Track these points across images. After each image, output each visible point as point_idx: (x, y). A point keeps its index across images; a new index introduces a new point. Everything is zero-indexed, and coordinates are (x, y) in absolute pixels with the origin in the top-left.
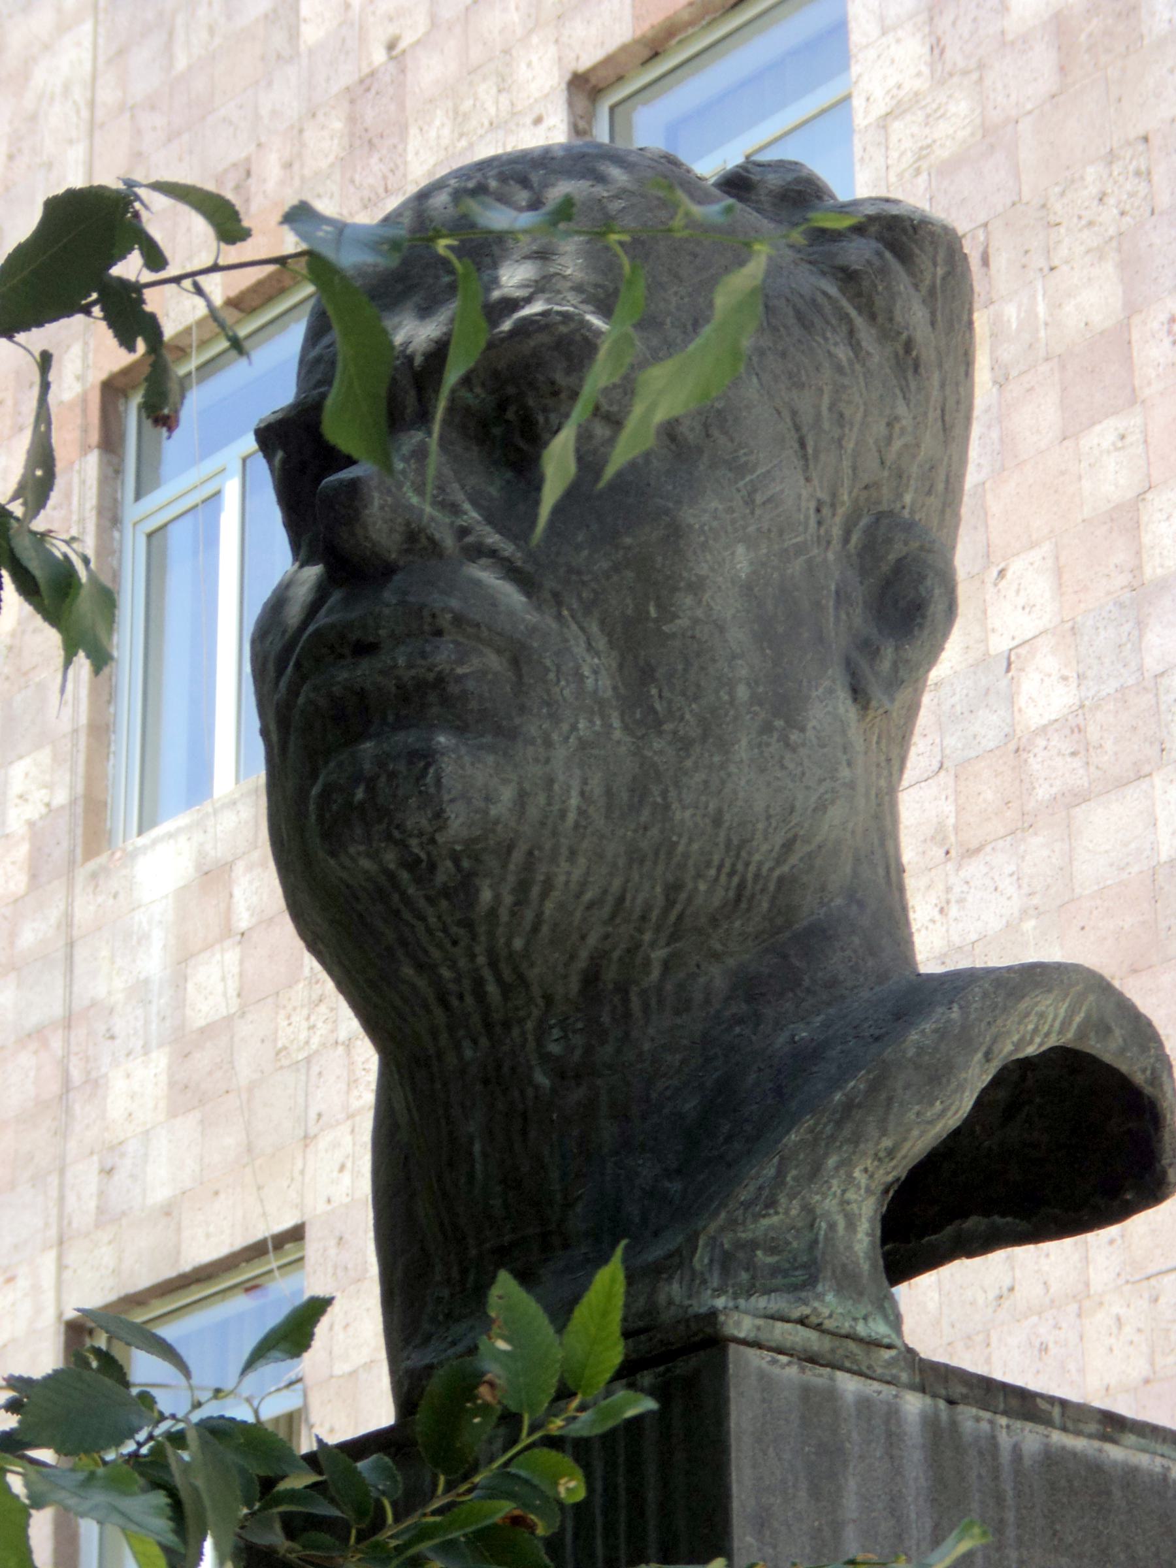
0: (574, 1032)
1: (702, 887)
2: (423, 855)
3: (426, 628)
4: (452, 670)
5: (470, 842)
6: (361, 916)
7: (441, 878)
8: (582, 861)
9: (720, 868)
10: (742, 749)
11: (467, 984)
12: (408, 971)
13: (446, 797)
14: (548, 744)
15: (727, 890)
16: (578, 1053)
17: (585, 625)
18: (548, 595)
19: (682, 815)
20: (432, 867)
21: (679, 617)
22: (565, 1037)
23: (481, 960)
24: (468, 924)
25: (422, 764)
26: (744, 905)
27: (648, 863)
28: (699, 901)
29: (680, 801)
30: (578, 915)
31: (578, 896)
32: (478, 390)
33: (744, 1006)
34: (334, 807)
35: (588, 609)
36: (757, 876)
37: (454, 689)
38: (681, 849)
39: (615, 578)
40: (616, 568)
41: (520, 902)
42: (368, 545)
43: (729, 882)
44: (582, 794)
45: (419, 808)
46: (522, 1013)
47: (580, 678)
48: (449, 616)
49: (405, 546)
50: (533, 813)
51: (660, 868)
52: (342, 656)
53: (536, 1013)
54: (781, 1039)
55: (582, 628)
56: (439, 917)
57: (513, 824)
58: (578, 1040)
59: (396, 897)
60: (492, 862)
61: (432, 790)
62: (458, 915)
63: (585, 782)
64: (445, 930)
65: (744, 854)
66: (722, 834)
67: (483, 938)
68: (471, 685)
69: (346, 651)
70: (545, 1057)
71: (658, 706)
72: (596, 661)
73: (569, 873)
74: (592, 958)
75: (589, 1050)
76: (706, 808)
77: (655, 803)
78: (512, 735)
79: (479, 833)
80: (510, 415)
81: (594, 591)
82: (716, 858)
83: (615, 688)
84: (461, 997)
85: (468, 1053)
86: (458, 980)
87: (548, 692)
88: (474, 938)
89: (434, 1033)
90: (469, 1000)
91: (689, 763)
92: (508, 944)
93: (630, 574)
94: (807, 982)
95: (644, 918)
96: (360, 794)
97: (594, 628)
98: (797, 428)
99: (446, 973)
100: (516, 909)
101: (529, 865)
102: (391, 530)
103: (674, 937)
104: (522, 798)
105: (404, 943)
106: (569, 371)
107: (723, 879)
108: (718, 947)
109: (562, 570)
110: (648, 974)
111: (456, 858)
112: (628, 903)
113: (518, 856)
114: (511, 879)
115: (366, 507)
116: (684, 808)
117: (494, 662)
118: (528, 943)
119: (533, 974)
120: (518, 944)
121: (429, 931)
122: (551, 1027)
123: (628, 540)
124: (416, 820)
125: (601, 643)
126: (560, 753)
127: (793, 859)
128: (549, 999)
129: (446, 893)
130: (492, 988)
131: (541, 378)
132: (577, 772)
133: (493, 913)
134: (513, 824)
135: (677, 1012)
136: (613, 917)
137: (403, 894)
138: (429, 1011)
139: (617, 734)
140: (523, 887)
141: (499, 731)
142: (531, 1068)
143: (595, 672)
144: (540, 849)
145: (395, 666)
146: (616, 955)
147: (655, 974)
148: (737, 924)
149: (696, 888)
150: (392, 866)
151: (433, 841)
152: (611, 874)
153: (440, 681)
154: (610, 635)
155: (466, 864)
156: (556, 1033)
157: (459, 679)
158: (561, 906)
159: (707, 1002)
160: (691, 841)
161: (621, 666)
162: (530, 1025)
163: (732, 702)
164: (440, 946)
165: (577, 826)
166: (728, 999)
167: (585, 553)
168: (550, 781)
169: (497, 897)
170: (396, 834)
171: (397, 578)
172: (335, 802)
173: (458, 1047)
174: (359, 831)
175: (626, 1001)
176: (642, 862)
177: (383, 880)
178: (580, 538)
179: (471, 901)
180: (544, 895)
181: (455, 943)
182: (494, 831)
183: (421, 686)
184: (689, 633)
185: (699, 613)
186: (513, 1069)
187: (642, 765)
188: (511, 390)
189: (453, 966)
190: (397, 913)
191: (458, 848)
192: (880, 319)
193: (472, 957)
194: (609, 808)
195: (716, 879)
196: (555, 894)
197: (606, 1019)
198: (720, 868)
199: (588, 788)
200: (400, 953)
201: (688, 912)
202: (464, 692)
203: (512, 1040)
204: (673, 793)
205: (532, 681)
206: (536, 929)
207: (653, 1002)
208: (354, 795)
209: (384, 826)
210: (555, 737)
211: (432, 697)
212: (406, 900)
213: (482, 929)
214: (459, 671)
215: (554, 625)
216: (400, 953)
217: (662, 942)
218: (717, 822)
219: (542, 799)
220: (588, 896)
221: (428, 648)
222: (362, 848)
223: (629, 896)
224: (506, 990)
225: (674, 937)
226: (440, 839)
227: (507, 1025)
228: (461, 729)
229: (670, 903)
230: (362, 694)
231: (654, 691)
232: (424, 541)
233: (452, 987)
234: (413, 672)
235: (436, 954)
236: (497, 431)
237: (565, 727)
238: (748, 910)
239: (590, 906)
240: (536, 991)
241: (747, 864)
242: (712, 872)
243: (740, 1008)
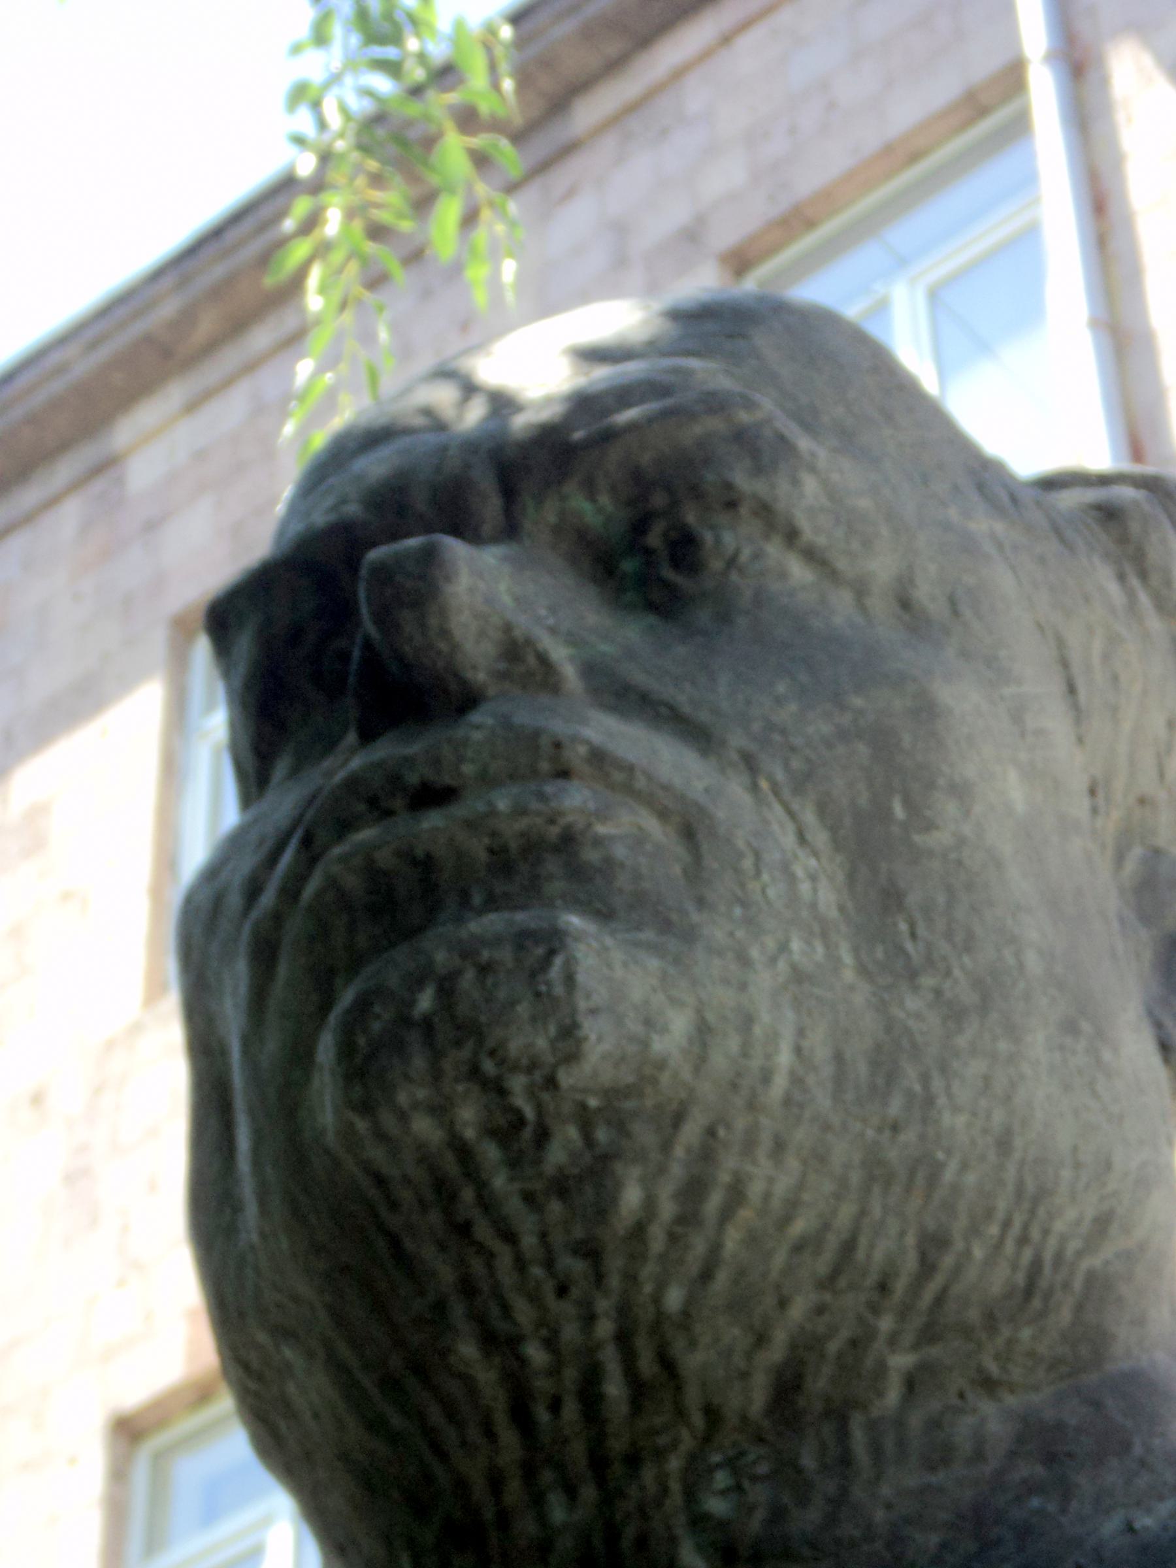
0: (754, 1479)
1: (978, 1253)
2: (529, 1113)
3: (545, 766)
4: (589, 825)
5: (613, 1094)
6: (395, 1242)
7: (556, 1156)
8: (793, 1163)
9: (1007, 1224)
10: (1038, 1041)
11: (571, 1375)
12: (468, 1350)
13: (582, 1005)
14: (744, 961)
15: (1015, 1267)
16: (760, 1515)
17: (795, 806)
18: (735, 757)
19: (954, 1122)
20: (543, 1136)
21: (937, 828)
22: (739, 1488)
23: (605, 1328)
24: (591, 1252)
25: (540, 951)
26: (1037, 1303)
27: (897, 1189)
28: (971, 1274)
29: (950, 1096)
30: (779, 1259)
31: (785, 1221)
32: (605, 500)
33: (1040, 1470)
34: (376, 1026)
35: (801, 782)
36: (1058, 1259)
37: (591, 855)
38: (948, 1175)
39: (841, 749)
40: (843, 735)
41: (688, 1218)
42: (443, 646)
43: (1018, 1254)
44: (798, 1050)
45: (534, 1019)
46: (663, 1440)
47: (792, 879)
48: (582, 750)
49: (502, 666)
50: (719, 1061)
51: (916, 1202)
52: (389, 813)
53: (687, 1442)
54: (1110, 1527)
55: (791, 814)
56: (543, 1235)
57: (686, 1074)
58: (759, 1494)
59: (468, 1194)
60: (645, 1135)
61: (559, 990)
62: (578, 1233)
63: (801, 1032)
64: (549, 1263)
65: (1041, 1212)
66: (1010, 1174)
67: (614, 1282)
68: (620, 852)
69: (398, 803)
70: (698, 1521)
71: (909, 946)
72: (813, 862)
73: (771, 1180)
74: (793, 1346)
75: (778, 1514)
76: (988, 1117)
77: (910, 1095)
78: (690, 935)
79: (630, 1079)
80: (654, 538)
81: (808, 760)
82: (1002, 1205)
83: (842, 909)
84: (555, 1406)
85: (558, 1513)
86: (554, 1371)
87: (742, 885)
88: (599, 1278)
89: (496, 1482)
90: (571, 1410)
91: (962, 1041)
92: (657, 1299)
93: (863, 749)
94: (1138, 1450)
95: (883, 1287)
96: (425, 1001)
97: (809, 817)
98: (1065, 664)
99: (536, 1354)
100: (679, 1230)
101: (707, 1154)
102: (482, 634)
103: (930, 1334)
104: (703, 1031)
105: (467, 1287)
106: (758, 470)
107: (1009, 1247)
108: (993, 1369)
109: (756, 726)
110: (880, 1394)
111: (585, 1120)
112: (860, 1255)
113: (691, 1132)
114: (677, 1171)
115: (448, 579)
116: (956, 1109)
117: (652, 825)
118: (691, 1301)
119: (692, 1362)
120: (674, 1298)
121: (520, 1264)
122: (712, 1469)
123: (858, 702)
124: (527, 1039)
125: (820, 838)
126: (764, 980)
127: (1108, 1251)
128: (712, 1414)
129: (561, 1187)
130: (614, 1389)
131: (710, 476)
132: (790, 1015)
133: (639, 1231)
134: (686, 1074)
135: (932, 1467)
136: (836, 1272)
137: (482, 1187)
138: (490, 1433)
139: (849, 975)
140: (694, 1190)
141: (666, 926)
142: (673, 1540)
143: (813, 878)
144: (728, 1127)
145: (493, 813)
146: (833, 1347)
147: (893, 1395)
148: (1026, 1333)
149: (968, 1253)
150: (470, 1134)
151: (551, 1083)
152: (838, 1196)
153: (568, 841)
154: (833, 830)
155: (602, 1135)
156: (722, 1479)
157: (598, 842)
158: (752, 1239)
159: (979, 1455)
160: (964, 1167)
161: (851, 877)
162: (674, 1464)
163: (1021, 966)
164: (535, 1298)
165: (787, 1101)
166: (1012, 1455)
167: (793, 707)
168: (748, 1021)
169: (650, 1204)
170: (489, 1067)
171: (485, 707)
172: (378, 1017)
173: (538, 1500)
174: (419, 1063)
175: (843, 1434)
176: (888, 1183)
177: (450, 1165)
178: (781, 688)
179: (603, 1210)
180: (726, 1214)
181: (562, 1291)
182: (654, 1081)
183: (533, 847)
184: (953, 856)
185: (967, 829)
186: (642, 1542)
187: (888, 1029)
188: (659, 500)
189: (551, 1343)
190: (464, 1230)
191: (593, 1102)
192: (1155, 580)
193: (589, 1319)
194: (839, 1081)
195: (999, 1246)
196: (745, 1214)
197: (808, 1461)
198: (1007, 1224)
199: (806, 1044)
200: (458, 1310)
201: (957, 1289)
202: (608, 861)
203: (642, 1488)
204: (937, 1084)
205: (715, 866)
206: (706, 1275)
207: (889, 1443)
208: (412, 1003)
209: (465, 1053)
210: (755, 953)
211: (552, 865)
212: (487, 1202)
213: (615, 1264)
214: (601, 829)
215: (747, 799)
216: (458, 1310)
217: (908, 1338)
218: (1004, 1144)
219: (734, 1044)
220: (799, 1226)
221: (549, 789)
222: (421, 1094)
223: (863, 1241)
224: (638, 1389)
225: (930, 1334)
226: (565, 1079)
227: (633, 1460)
228: (604, 915)
229: (927, 1268)
230: (426, 865)
231: (903, 927)
232: (532, 660)
233: (542, 1384)
234: (522, 824)
235: (524, 1313)
236: (629, 566)
237: (771, 943)
238: (1043, 1314)
239: (798, 1248)
240: (693, 1397)
241: (1046, 1232)
242: (994, 1230)
243: (1029, 1469)
